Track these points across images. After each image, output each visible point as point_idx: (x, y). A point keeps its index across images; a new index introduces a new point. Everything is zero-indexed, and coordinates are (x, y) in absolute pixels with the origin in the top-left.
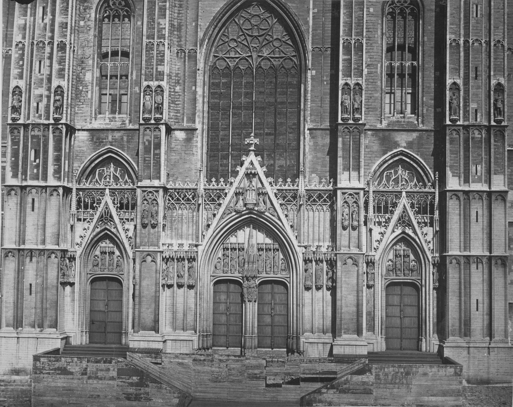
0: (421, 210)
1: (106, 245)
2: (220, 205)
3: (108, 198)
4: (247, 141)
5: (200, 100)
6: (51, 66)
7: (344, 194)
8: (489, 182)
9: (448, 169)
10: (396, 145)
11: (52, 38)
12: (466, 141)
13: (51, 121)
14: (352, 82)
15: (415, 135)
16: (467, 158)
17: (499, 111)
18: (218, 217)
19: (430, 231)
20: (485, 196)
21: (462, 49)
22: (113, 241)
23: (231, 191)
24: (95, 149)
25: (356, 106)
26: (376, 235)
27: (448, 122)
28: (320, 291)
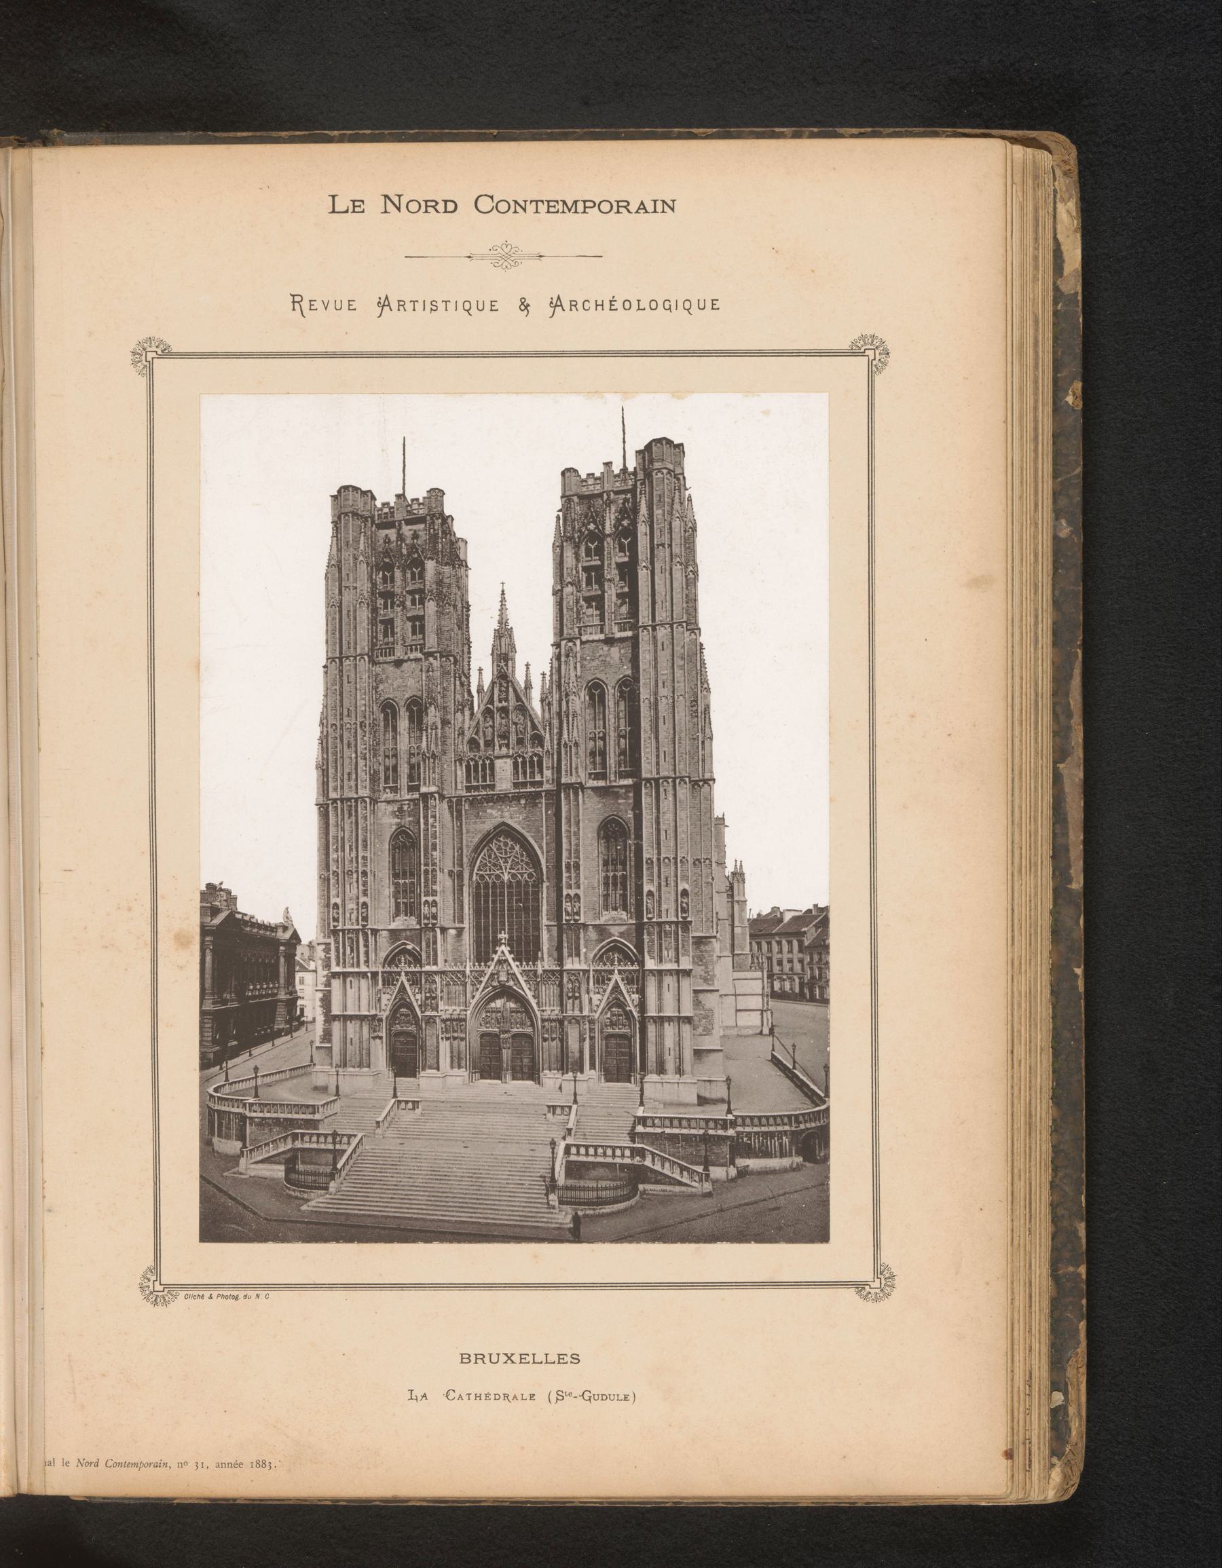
0: (629, 982)
2: (481, 982)
3: (403, 978)
6: (358, 888)
8: (677, 961)
10: (611, 935)
13: (360, 927)
23: (489, 971)
24: (393, 943)
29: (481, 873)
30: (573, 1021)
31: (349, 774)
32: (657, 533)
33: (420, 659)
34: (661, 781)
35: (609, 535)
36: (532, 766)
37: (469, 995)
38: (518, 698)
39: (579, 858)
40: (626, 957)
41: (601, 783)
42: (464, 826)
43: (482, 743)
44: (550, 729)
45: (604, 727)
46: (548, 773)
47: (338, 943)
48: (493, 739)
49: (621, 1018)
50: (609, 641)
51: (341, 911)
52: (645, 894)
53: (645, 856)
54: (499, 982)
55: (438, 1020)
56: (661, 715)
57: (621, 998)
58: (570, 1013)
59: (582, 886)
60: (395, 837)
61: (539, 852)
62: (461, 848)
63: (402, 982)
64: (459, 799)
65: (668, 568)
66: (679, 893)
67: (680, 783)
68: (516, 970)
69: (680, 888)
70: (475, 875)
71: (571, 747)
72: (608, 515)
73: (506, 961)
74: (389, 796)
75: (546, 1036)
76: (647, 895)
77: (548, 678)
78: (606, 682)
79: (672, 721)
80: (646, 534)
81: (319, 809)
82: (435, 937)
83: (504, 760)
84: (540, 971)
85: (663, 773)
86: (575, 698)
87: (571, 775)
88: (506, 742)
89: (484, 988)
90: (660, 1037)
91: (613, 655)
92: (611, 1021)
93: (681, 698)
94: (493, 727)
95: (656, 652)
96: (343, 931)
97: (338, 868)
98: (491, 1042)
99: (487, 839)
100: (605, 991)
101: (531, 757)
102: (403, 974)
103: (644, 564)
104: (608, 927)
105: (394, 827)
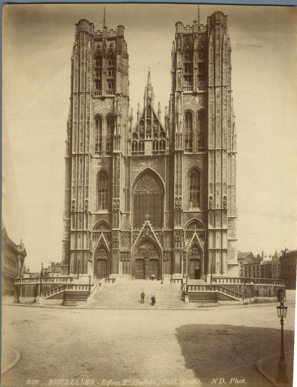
0: (201, 236)
1: (102, 250)
2: (137, 236)
3: (102, 235)
4: (146, 216)
5: (131, 204)
6: (84, 194)
7: (176, 231)
8: (222, 227)
9: (209, 223)
14: (178, 197)
16: (215, 219)
17: (225, 205)
18: (137, 239)
20: (220, 231)
21: (213, 186)
24: (97, 220)
25: (180, 204)
27: (209, 209)
28: (169, 261)
29: (137, 190)
30: (178, 252)
31: (81, 144)
32: (216, 50)
33: (114, 97)
34: (216, 151)
35: (196, 50)
36: (161, 145)
39: (181, 182)
40: (199, 226)
41: (190, 153)
42: (131, 169)
43: (139, 135)
44: (169, 130)
46: (167, 148)
48: (144, 133)
49: (196, 252)
50: (195, 94)
51: (76, 204)
52: (209, 198)
54: (145, 236)
56: (217, 124)
57: (197, 243)
58: (176, 248)
59: (182, 194)
61: (163, 181)
62: (129, 179)
63: (102, 236)
64: (129, 158)
65: (221, 64)
66: (223, 198)
67: (224, 152)
68: (152, 231)
69: (223, 196)
70: (134, 191)
71: (179, 135)
72: (195, 42)
73: (149, 226)
75: (165, 259)
76: (210, 198)
77: (168, 109)
78: (194, 111)
79: (221, 127)
80: (212, 50)
81: (66, 160)
82: (118, 216)
83: (149, 142)
85: (217, 148)
86: (180, 116)
87: (179, 147)
88: (150, 134)
89: (139, 238)
90: (214, 258)
91: (196, 100)
92: (192, 253)
93: (225, 117)
94: (144, 128)
95: (215, 98)
96: (77, 213)
97: (75, 185)
101: (161, 141)
102: (102, 233)
103: (211, 62)
104: (192, 213)
105: (99, 169)
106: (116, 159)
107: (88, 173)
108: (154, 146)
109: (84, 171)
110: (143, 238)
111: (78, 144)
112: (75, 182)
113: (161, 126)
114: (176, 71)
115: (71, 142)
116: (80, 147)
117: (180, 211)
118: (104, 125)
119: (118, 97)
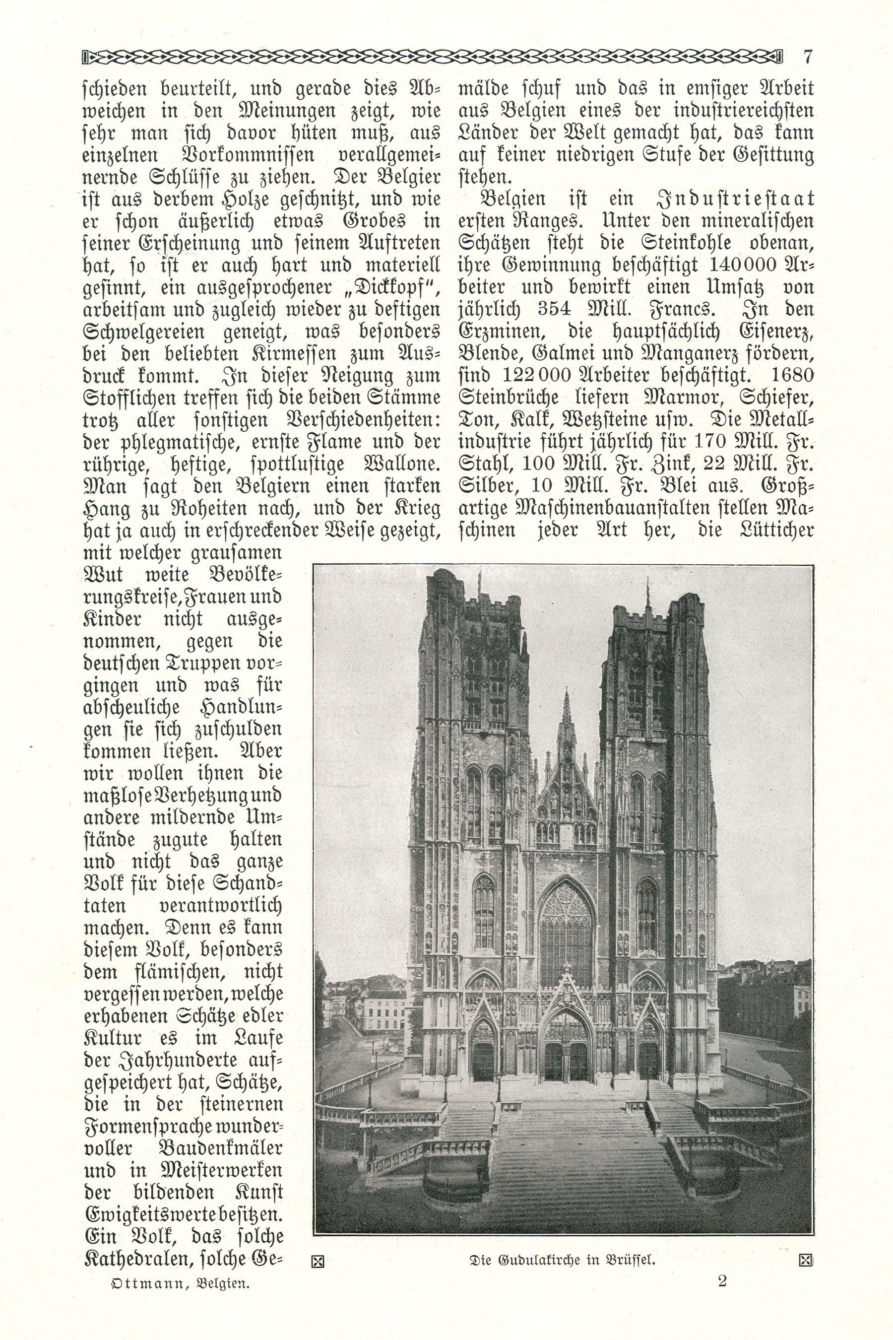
3: (484, 999)
5: (535, 940)
6: (449, 920)
10: (645, 967)
11: (449, 903)
12: (685, 965)
15: (654, 962)
18: (549, 1008)
19: (663, 1015)
22: (488, 1023)
23: (556, 994)
26: (635, 1018)
36: (589, 834)
37: (540, 1013)
38: (577, 780)
43: (549, 810)
45: (642, 809)
46: (600, 840)
47: (430, 967)
50: (648, 744)
51: (434, 939)
53: (675, 908)
55: (516, 1033)
58: (620, 1027)
60: (478, 881)
68: (578, 994)
74: (474, 846)
84: (595, 994)
96: (435, 956)
98: (555, 1051)
99: (553, 887)
100: (641, 1010)
102: (484, 995)
105: (478, 873)
106: (510, 857)
107: (456, 880)
108: (576, 834)
109: (449, 875)
110: (561, 1006)
111: (437, 822)
112: (431, 896)
113: (588, 798)
114: (616, 697)
115: (422, 814)
116: (440, 828)
117: (626, 960)
118: (486, 787)
119: (513, 735)
